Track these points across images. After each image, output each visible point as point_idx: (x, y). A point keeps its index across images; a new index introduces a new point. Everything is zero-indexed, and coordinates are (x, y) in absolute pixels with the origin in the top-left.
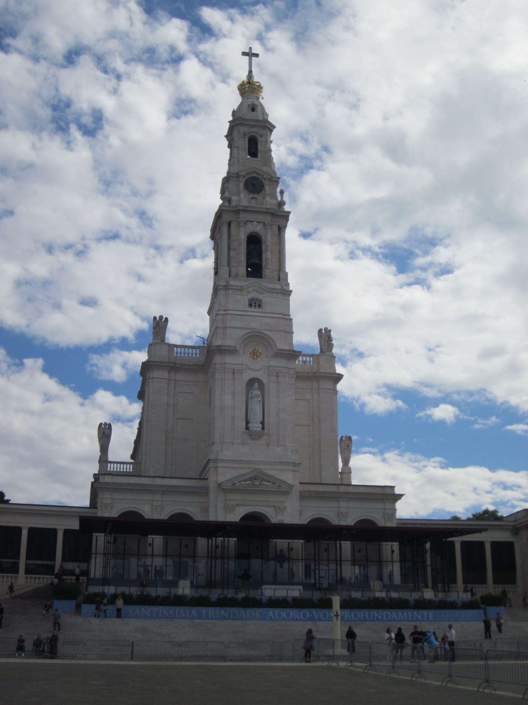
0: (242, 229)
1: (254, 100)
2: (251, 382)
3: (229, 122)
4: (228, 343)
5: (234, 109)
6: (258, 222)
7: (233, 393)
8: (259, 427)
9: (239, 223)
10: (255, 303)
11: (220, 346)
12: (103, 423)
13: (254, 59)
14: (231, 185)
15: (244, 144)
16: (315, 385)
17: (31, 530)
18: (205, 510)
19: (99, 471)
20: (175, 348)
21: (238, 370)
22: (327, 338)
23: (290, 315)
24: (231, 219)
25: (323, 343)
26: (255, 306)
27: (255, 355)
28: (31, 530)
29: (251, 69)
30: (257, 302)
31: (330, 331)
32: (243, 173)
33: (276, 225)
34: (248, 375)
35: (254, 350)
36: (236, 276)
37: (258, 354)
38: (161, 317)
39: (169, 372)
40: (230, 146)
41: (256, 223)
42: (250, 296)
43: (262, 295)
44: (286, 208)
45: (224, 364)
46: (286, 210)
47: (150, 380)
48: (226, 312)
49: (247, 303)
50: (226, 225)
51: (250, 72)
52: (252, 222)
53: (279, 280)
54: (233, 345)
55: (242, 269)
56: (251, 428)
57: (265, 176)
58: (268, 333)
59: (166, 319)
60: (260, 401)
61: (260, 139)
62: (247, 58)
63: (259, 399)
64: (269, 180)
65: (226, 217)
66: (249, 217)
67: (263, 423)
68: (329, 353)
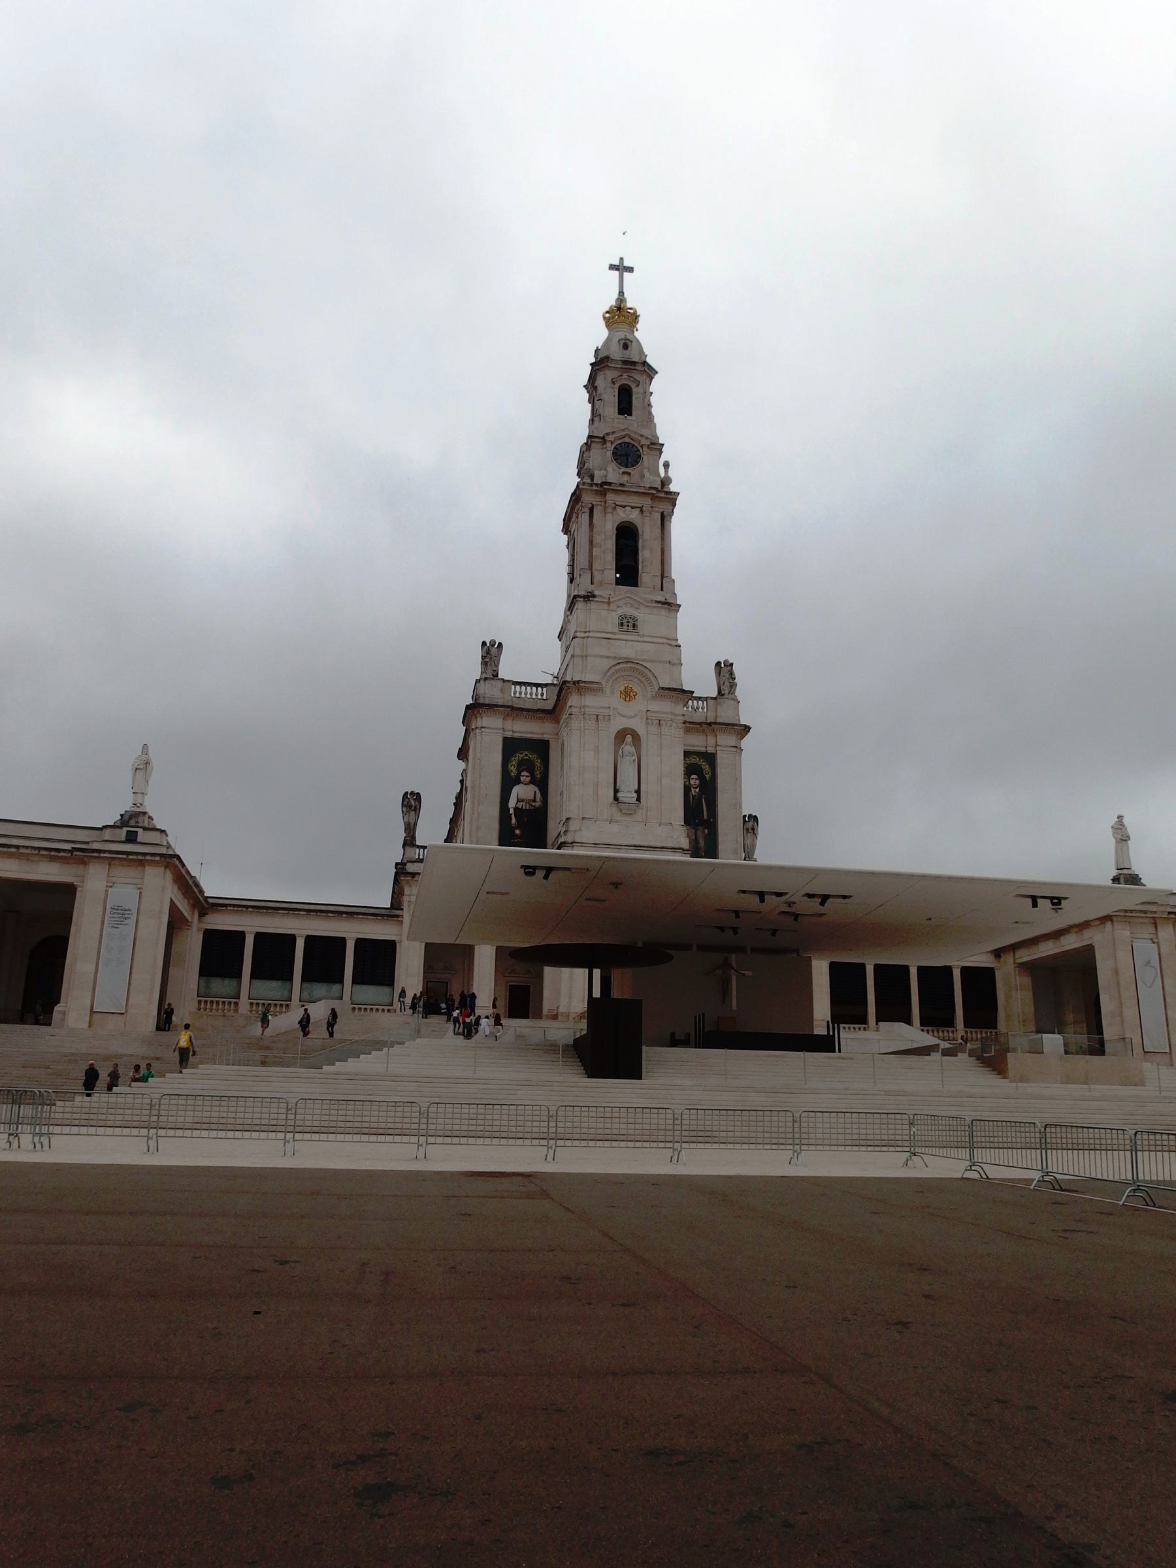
0: (609, 516)
1: (627, 334)
2: (621, 736)
3: (591, 364)
5: (597, 347)
6: (633, 508)
7: (597, 750)
8: (633, 797)
9: (605, 508)
10: (628, 624)
11: (578, 682)
12: (409, 792)
13: (626, 274)
14: (596, 451)
15: (611, 398)
17: (309, 939)
20: (513, 687)
21: (603, 716)
22: (727, 675)
23: (677, 640)
24: (594, 503)
25: (722, 683)
26: (628, 626)
27: (628, 695)
28: (309, 939)
29: (623, 290)
30: (630, 620)
31: (732, 665)
32: (611, 438)
33: (658, 512)
34: (618, 724)
36: (601, 583)
38: (493, 643)
39: (504, 719)
40: (592, 400)
41: (630, 508)
42: (621, 612)
43: (638, 611)
44: (673, 488)
45: (584, 706)
46: (671, 490)
47: (477, 730)
48: (587, 635)
49: (616, 621)
50: (587, 510)
51: (621, 293)
52: (624, 507)
53: (662, 590)
55: (611, 575)
56: (621, 799)
57: (643, 442)
59: (500, 645)
61: (635, 389)
62: (617, 273)
63: (633, 758)
64: (648, 447)
65: (588, 499)
66: (620, 499)
67: (638, 792)
68: (730, 696)
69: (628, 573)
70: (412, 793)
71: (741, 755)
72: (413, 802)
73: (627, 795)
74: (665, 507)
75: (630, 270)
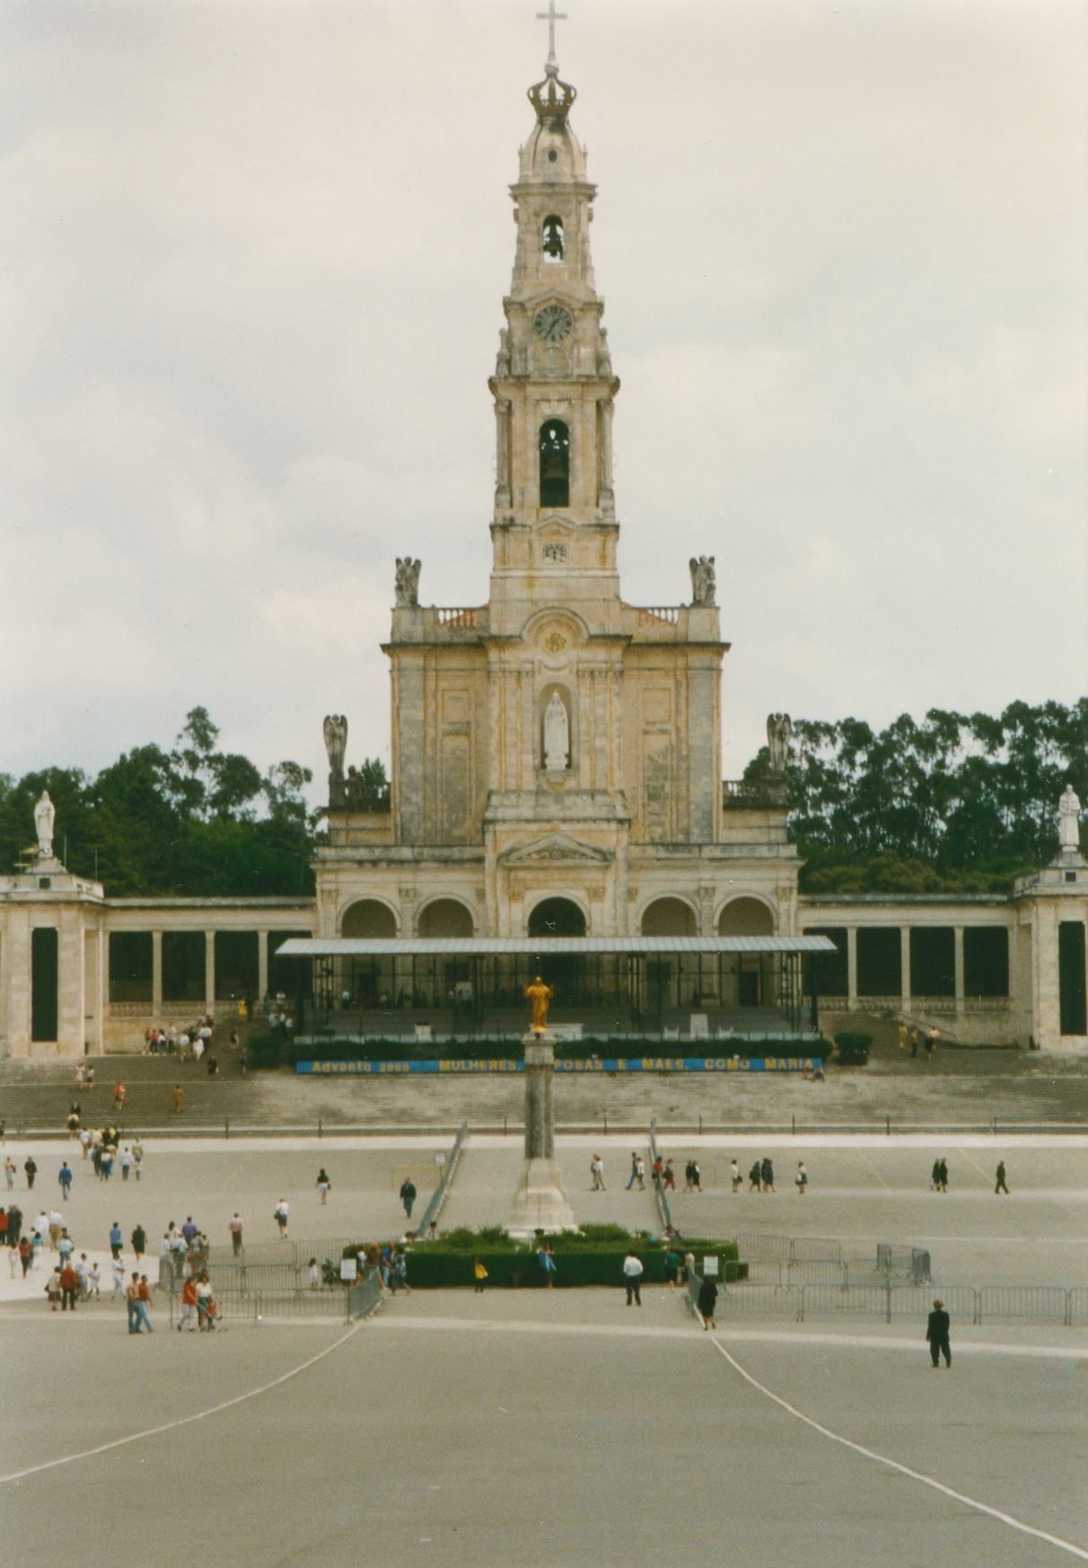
2: (550, 688)
4: (511, 628)
5: (521, 146)
10: (554, 552)
13: (557, 22)
16: (681, 662)
18: (481, 895)
19: (331, 801)
26: (555, 558)
27: (555, 643)
31: (712, 560)
35: (553, 635)
37: (560, 642)
38: (408, 561)
39: (425, 657)
51: (552, 54)
54: (517, 634)
56: (548, 768)
58: (573, 606)
59: (418, 563)
60: (563, 721)
62: (546, 22)
69: (555, 490)
70: (336, 718)
71: (719, 676)
72: (340, 731)
73: (556, 761)
74: (602, 392)
75: (563, 16)
